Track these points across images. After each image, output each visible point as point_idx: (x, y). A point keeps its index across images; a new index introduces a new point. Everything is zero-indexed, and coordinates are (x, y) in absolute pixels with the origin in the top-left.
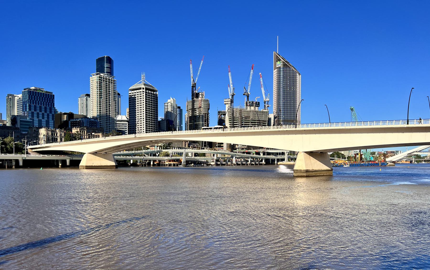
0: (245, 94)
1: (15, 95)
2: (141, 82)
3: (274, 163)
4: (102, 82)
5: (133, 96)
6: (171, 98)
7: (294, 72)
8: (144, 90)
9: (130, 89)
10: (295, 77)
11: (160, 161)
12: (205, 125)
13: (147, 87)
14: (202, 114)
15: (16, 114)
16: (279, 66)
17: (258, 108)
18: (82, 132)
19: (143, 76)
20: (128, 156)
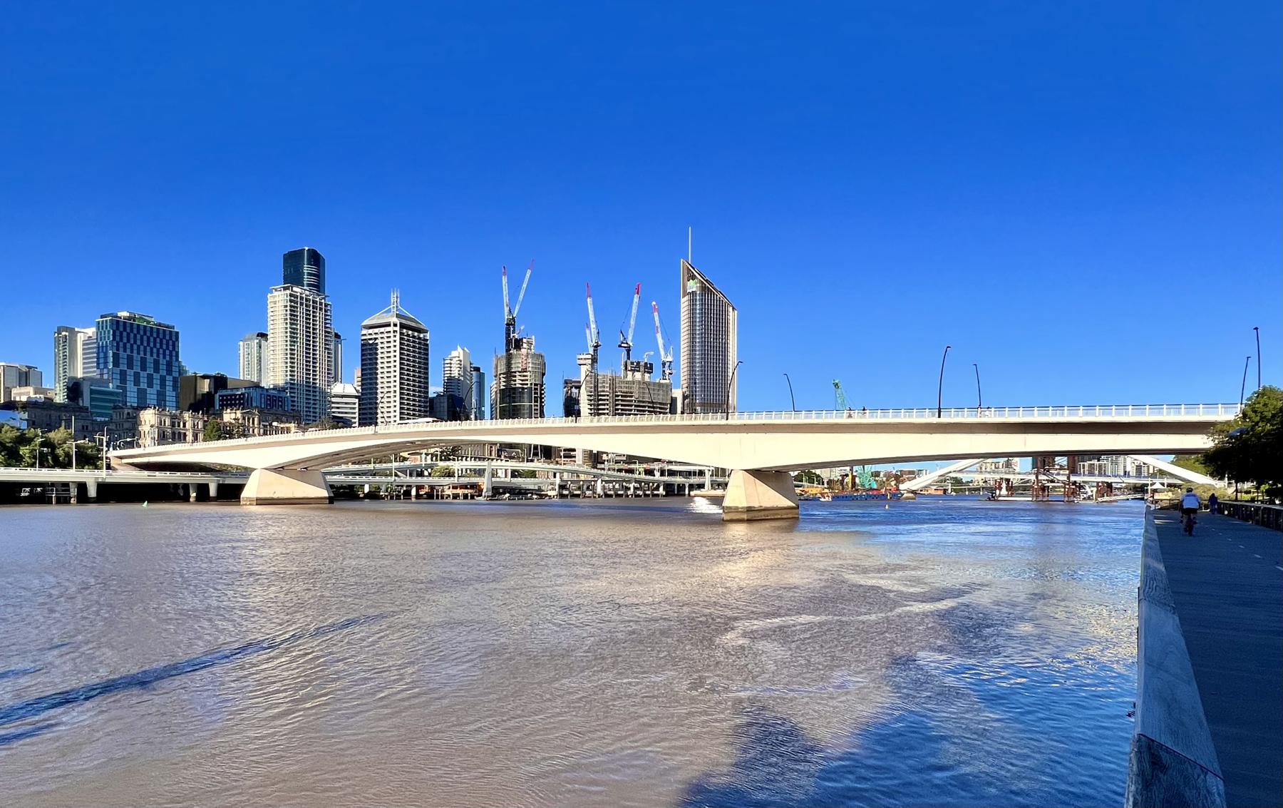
0: (623, 345)
1: (76, 329)
2: (389, 311)
3: (682, 493)
4: (297, 308)
5: (371, 342)
6: (459, 349)
9: (363, 324)
11: (432, 488)
12: (536, 408)
13: (404, 321)
14: (529, 386)
15: (80, 375)
16: (694, 290)
17: (649, 375)
18: (249, 419)
19: (394, 298)
20: (358, 475)
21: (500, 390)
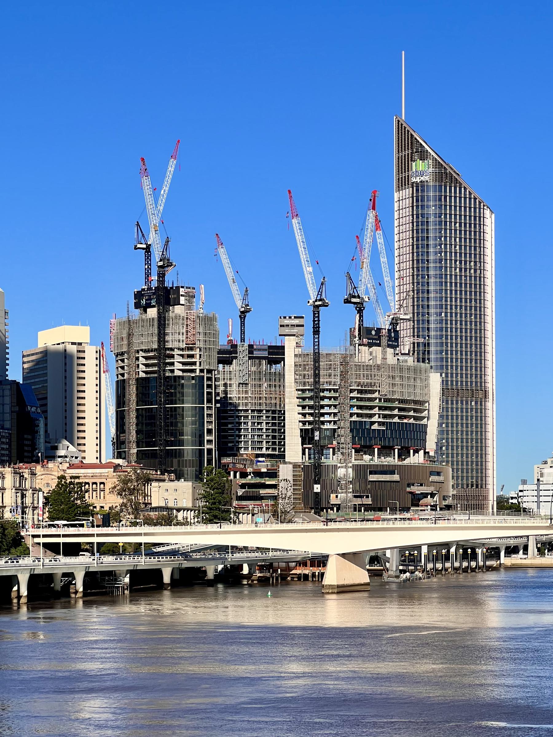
0: (354, 300)
7: (475, 202)
10: (479, 221)
16: (422, 178)
21: (137, 380)
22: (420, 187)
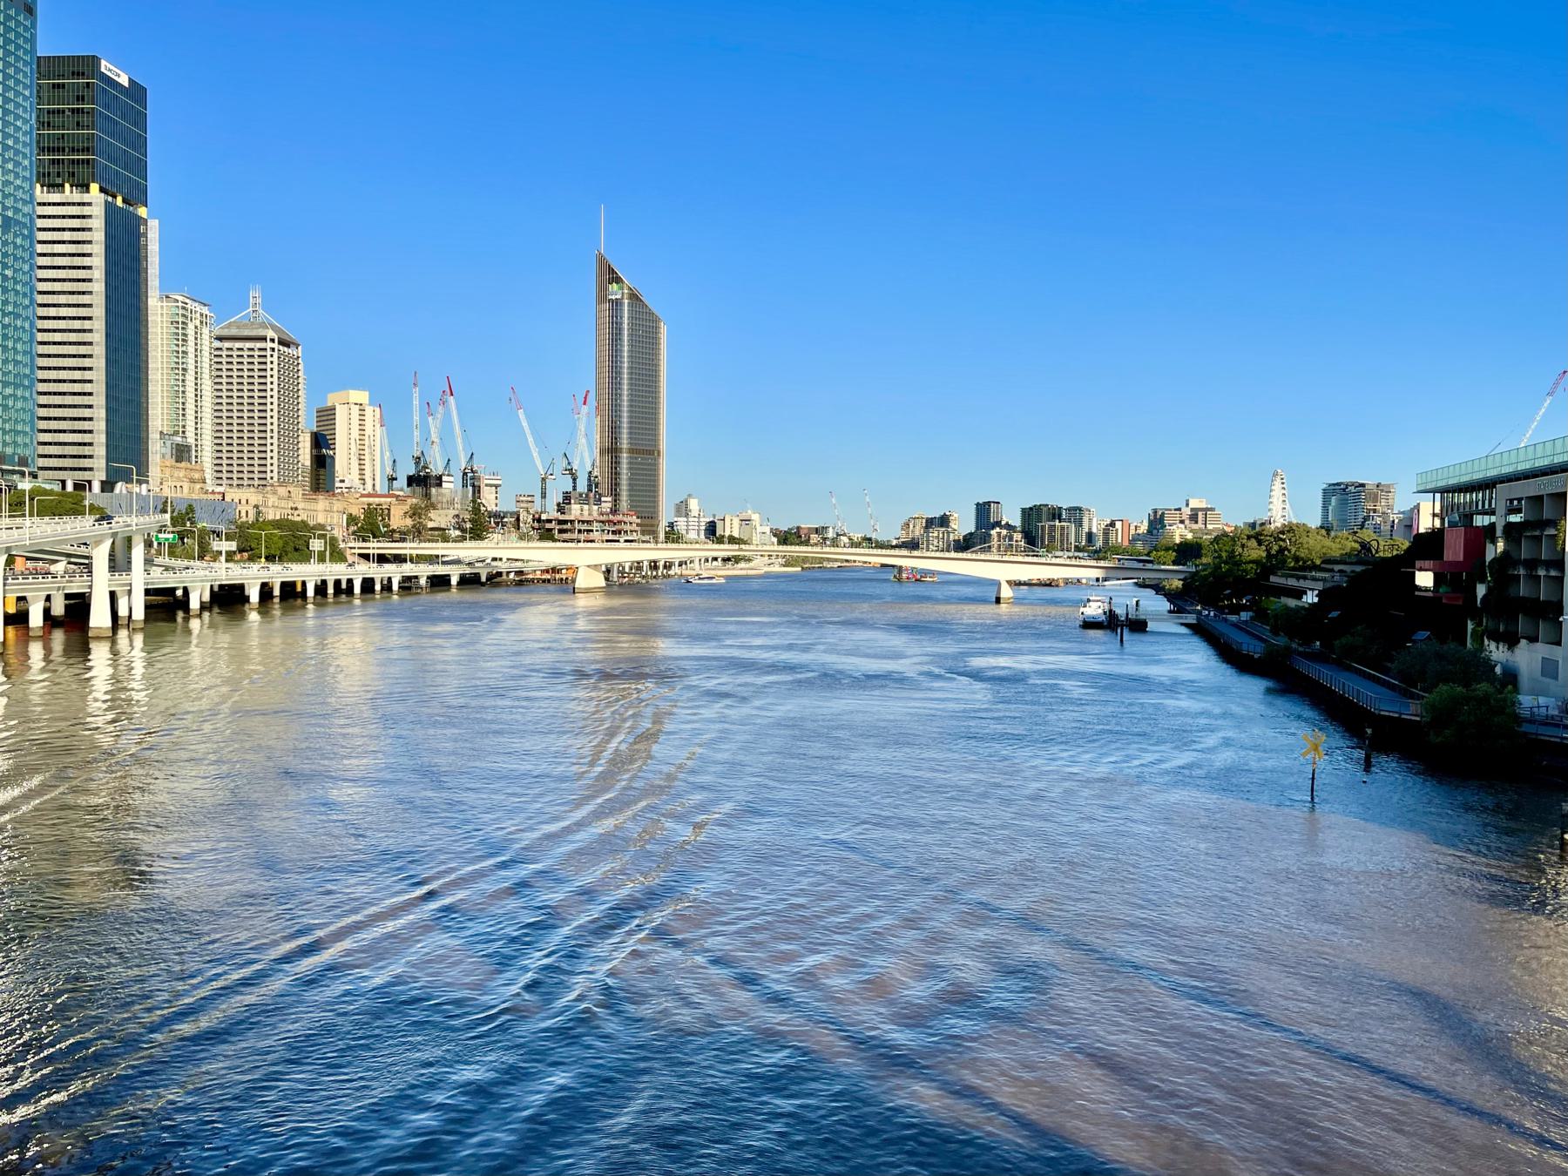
8: (272, 345)
19: (255, 295)
22: (617, 304)
